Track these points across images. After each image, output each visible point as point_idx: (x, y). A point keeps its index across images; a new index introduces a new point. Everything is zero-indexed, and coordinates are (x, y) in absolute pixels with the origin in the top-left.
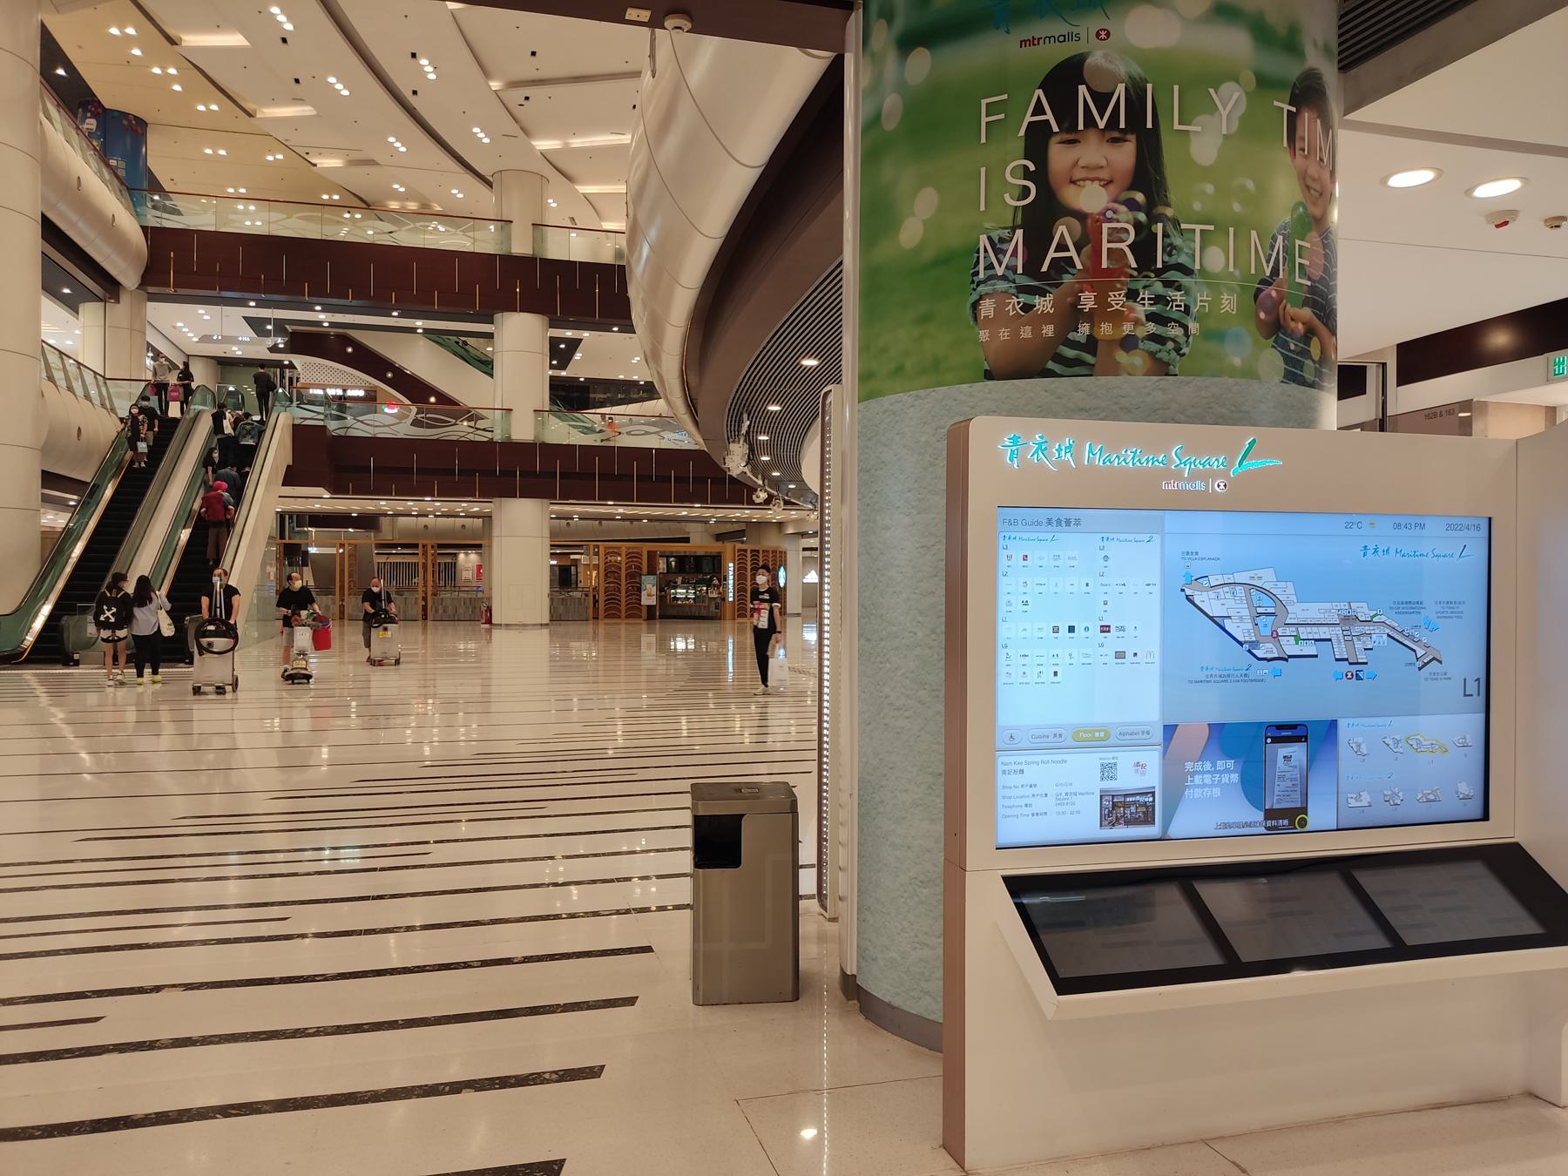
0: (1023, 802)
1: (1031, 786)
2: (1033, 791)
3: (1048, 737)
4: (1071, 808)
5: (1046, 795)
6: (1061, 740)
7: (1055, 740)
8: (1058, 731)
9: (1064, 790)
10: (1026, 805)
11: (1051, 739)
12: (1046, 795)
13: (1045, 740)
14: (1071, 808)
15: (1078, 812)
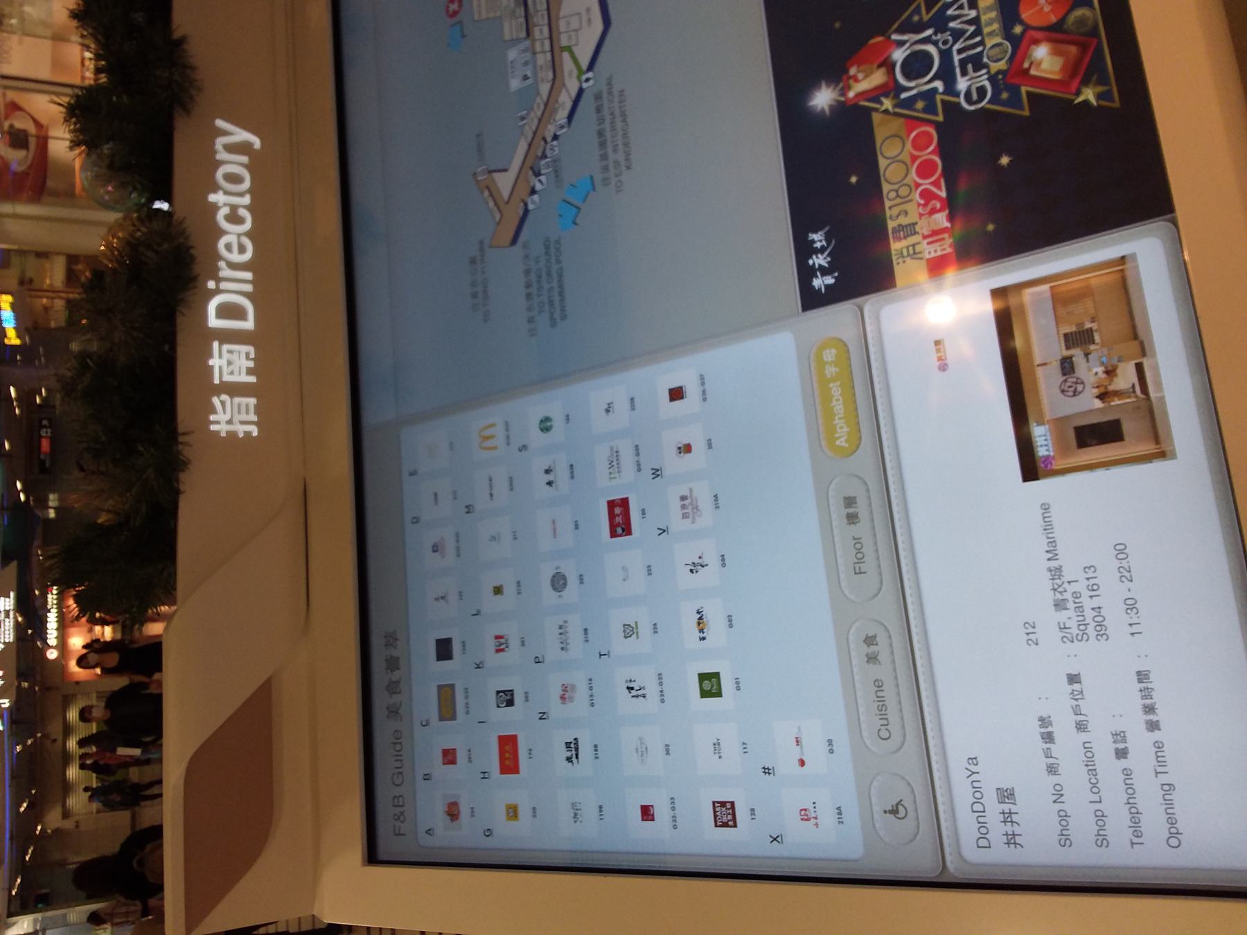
0: (1109, 767)
1: (1049, 738)
2: (1063, 726)
3: (879, 685)
4: (1107, 577)
5: (1073, 679)
6: (882, 639)
7: (884, 656)
8: (858, 651)
9: (1049, 620)
10: (1121, 754)
11: (882, 671)
12: (1073, 679)
13: (889, 693)
14: (1107, 577)
15: (1121, 551)
